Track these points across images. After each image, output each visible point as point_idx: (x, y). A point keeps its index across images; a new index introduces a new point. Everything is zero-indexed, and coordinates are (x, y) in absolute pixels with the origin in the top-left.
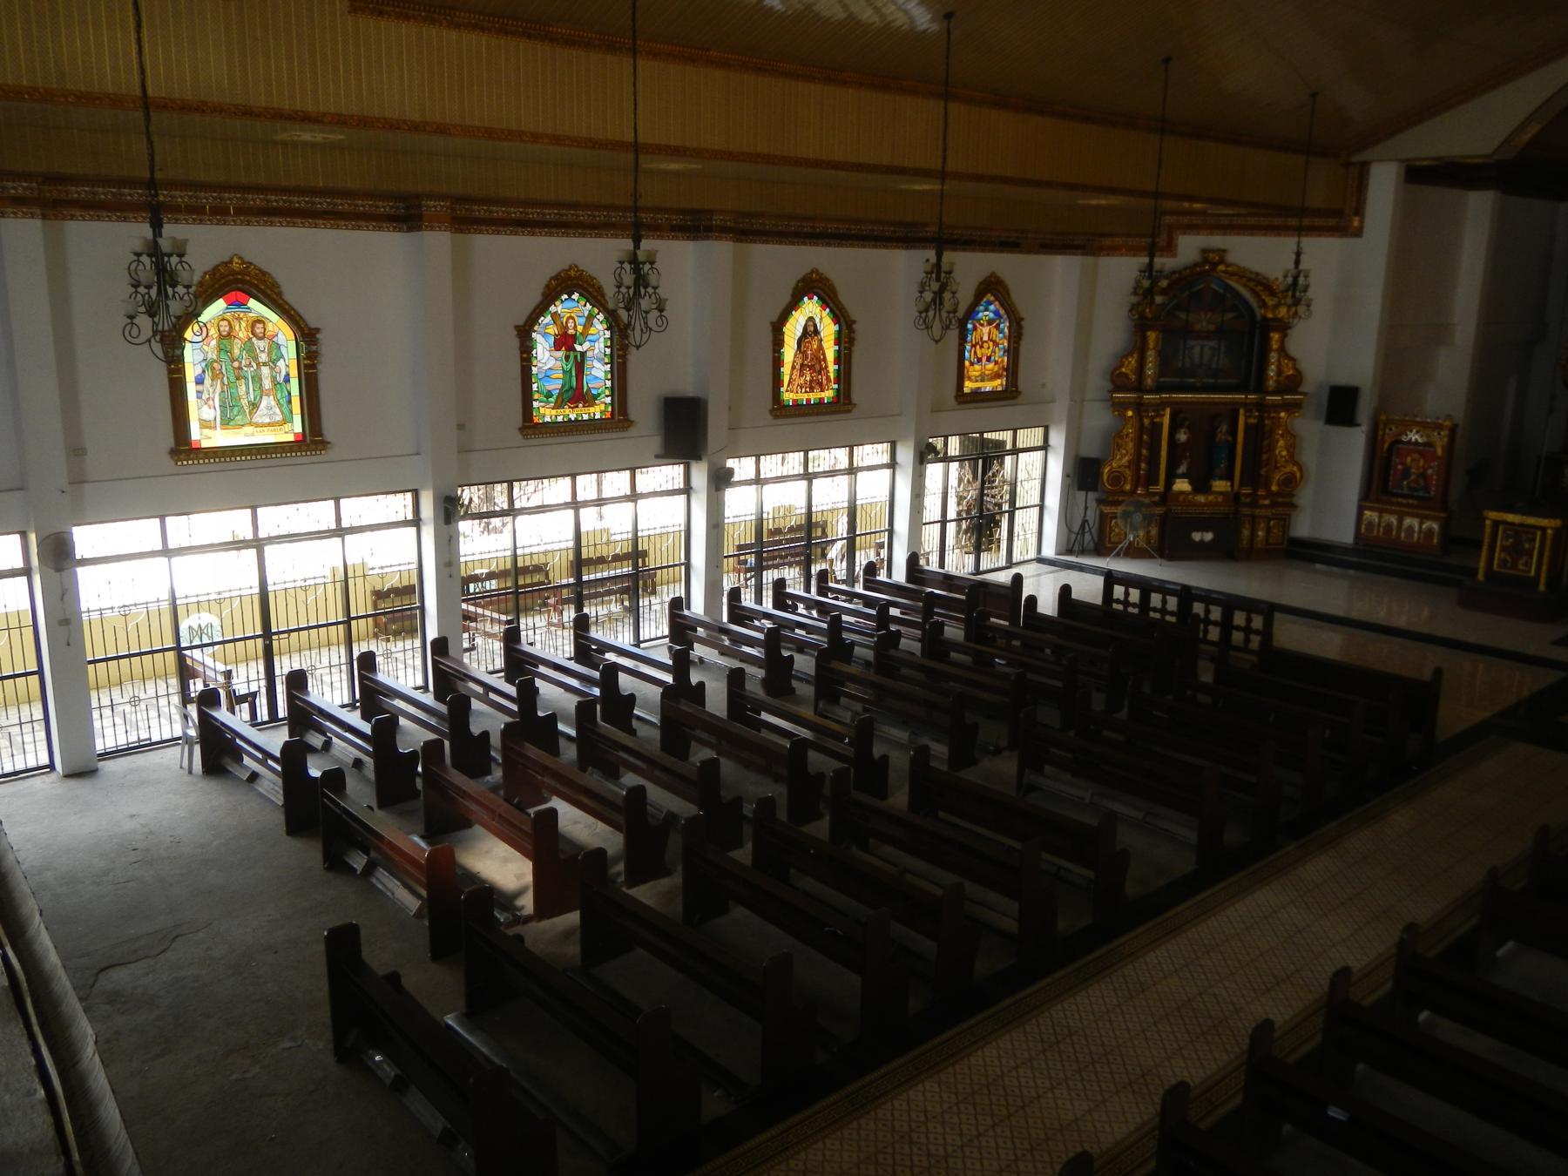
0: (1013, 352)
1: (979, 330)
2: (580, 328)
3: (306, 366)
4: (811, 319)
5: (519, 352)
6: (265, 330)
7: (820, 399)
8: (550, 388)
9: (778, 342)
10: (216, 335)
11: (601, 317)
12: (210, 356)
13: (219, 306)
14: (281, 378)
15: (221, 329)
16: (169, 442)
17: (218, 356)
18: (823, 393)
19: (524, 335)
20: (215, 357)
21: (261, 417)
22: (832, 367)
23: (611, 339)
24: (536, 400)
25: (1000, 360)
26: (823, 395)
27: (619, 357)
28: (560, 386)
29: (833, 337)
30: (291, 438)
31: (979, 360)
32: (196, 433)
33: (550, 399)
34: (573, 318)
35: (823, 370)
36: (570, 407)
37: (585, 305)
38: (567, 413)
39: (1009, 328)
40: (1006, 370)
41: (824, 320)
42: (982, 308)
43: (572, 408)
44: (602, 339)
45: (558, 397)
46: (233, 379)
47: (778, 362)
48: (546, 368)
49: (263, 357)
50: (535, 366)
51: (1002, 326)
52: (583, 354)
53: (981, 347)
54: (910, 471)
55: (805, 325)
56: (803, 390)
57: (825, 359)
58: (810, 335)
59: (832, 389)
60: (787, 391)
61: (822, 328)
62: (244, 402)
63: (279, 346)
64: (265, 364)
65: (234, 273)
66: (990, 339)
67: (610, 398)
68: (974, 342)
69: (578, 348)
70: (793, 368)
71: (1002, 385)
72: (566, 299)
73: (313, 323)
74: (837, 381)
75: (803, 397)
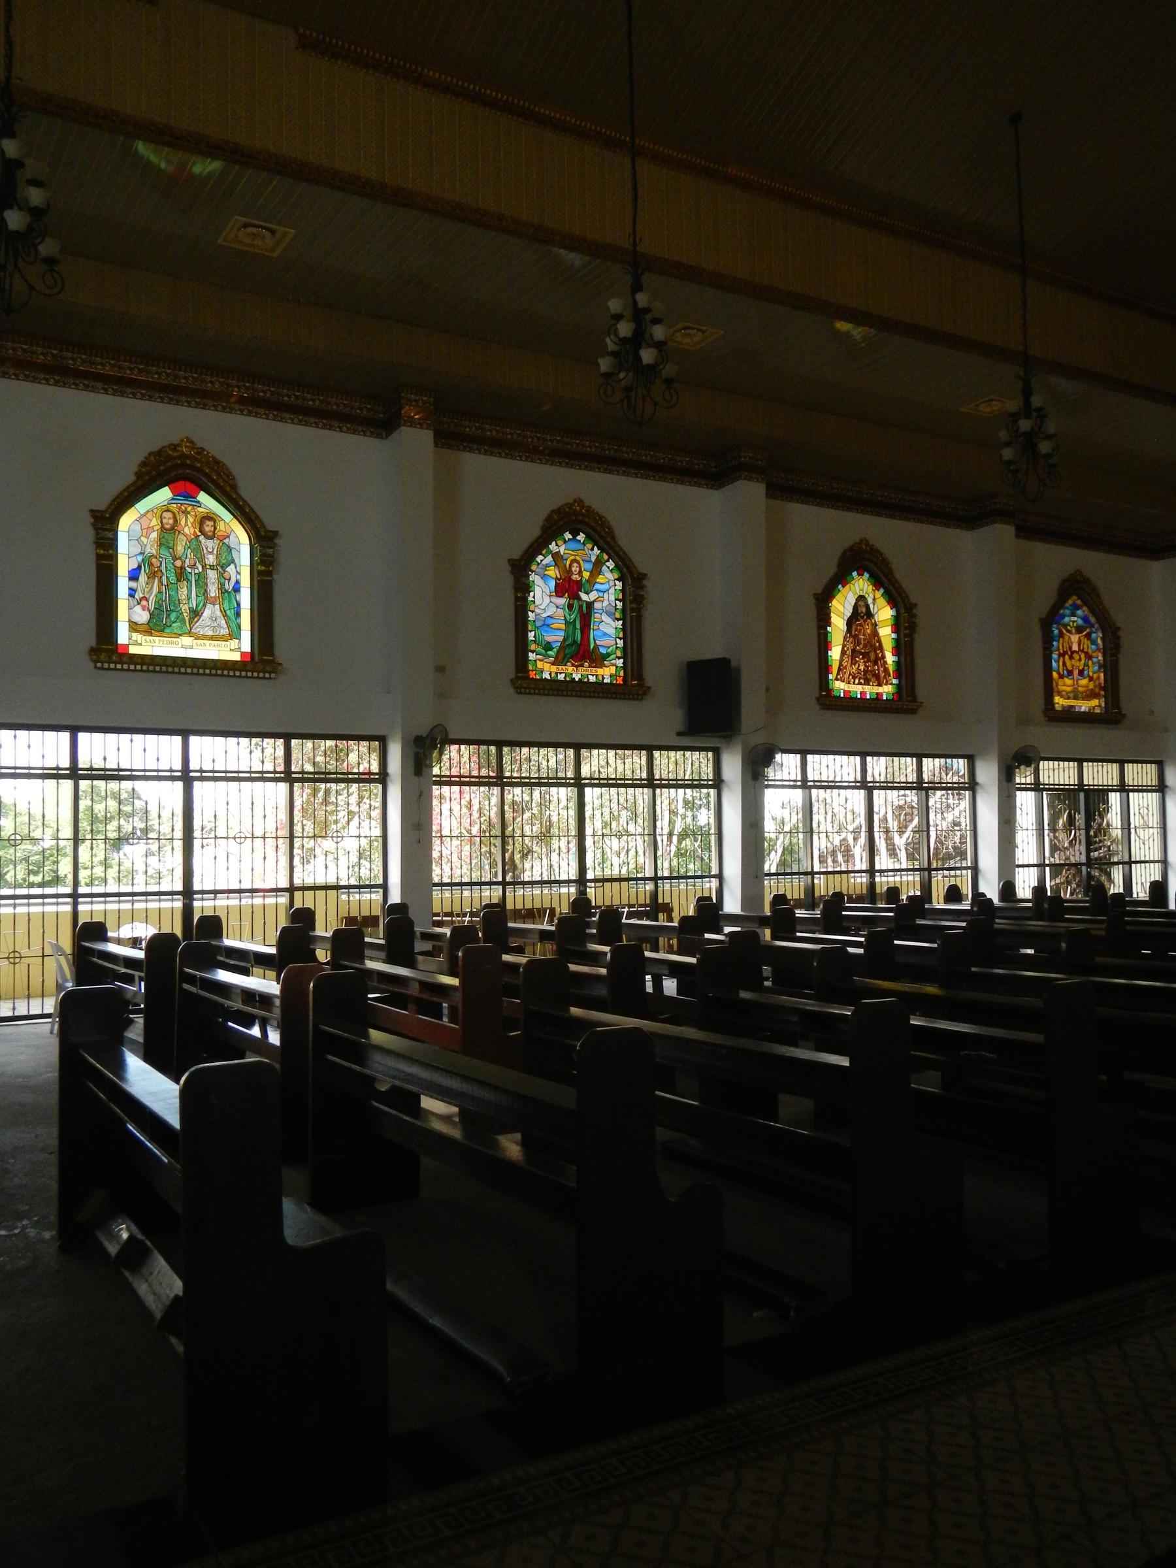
0: (1111, 667)
1: (1066, 638)
3: (260, 573)
4: (861, 598)
5: (513, 591)
6: (215, 529)
7: (877, 694)
8: (550, 639)
9: (824, 619)
10: (158, 527)
11: (611, 564)
12: (148, 550)
13: (164, 494)
14: (229, 587)
15: (165, 521)
16: (91, 640)
17: (158, 551)
19: (520, 570)
20: (154, 552)
21: (203, 627)
22: (890, 659)
23: (623, 591)
25: (1095, 676)
26: (881, 690)
27: (632, 610)
28: (561, 639)
29: (891, 622)
30: (236, 657)
31: (1070, 673)
32: (123, 635)
33: (549, 653)
34: (578, 562)
36: (573, 665)
37: (592, 549)
38: (570, 671)
39: (1103, 639)
40: (1104, 689)
42: (1067, 612)
43: (577, 667)
44: (612, 591)
45: (558, 652)
46: (173, 579)
47: (824, 645)
48: (545, 615)
49: (211, 559)
50: (532, 612)
51: (1094, 635)
52: (590, 605)
53: (1071, 658)
54: (994, 790)
55: (856, 604)
56: (857, 681)
57: (881, 647)
58: (862, 617)
59: (891, 684)
60: (837, 679)
63: (230, 549)
64: (212, 567)
65: (184, 456)
66: (1081, 650)
67: (622, 660)
69: (584, 597)
70: (843, 653)
71: (1100, 706)
72: (569, 539)
73: (271, 526)
74: (898, 673)
75: (856, 689)
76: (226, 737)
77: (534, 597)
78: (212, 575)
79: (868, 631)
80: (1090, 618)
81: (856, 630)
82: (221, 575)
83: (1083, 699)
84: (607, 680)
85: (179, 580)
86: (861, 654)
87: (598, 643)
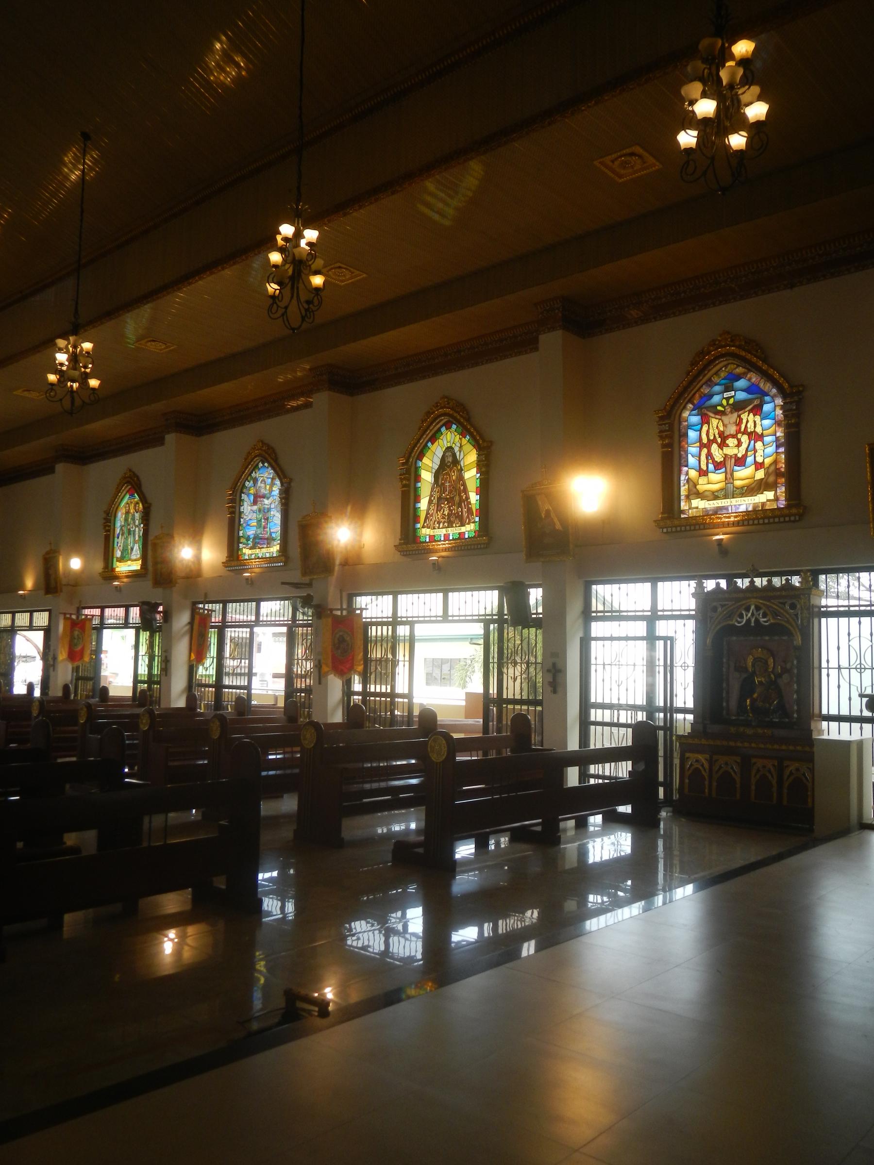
4: (450, 449)
7: (460, 534)
18: (462, 528)
21: (133, 555)
22: (474, 498)
24: (241, 543)
26: (463, 529)
38: (257, 552)
41: (464, 448)
50: (242, 518)
57: (465, 490)
58: (449, 467)
59: (474, 522)
60: (423, 527)
61: (462, 457)
62: (129, 547)
70: (430, 502)
72: (261, 467)
77: (244, 509)
78: (137, 529)
79: (454, 478)
80: (761, 385)
81: (442, 480)
82: (139, 528)
83: (743, 495)
84: (275, 555)
85: (129, 535)
86: (446, 499)
87: (272, 530)
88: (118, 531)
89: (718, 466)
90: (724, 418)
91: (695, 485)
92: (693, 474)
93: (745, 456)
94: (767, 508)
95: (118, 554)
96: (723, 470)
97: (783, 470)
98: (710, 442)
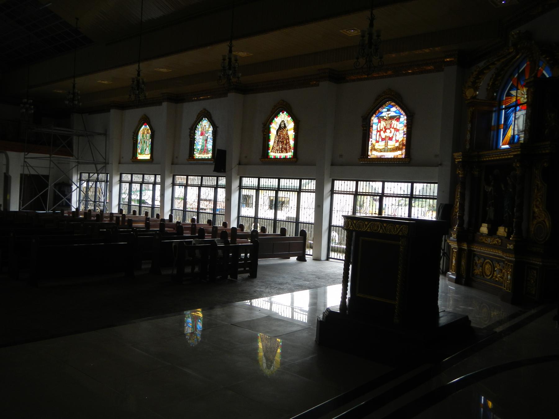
2: (207, 129)
4: (283, 121)
7: (285, 156)
9: (267, 132)
22: (292, 143)
26: (286, 154)
28: (201, 147)
33: (198, 151)
35: (288, 143)
42: (385, 110)
55: (280, 124)
56: (278, 152)
57: (288, 139)
58: (282, 128)
59: (292, 152)
60: (271, 152)
62: (144, 149)
68: (379, 129)
70: (275, 142)
75: (278, 155)
76: (350, 181)
78: (148, 141)
79: (284, 133)
81: (280, 134)
82: (149, 141)
83: (390, 151)
86: (281, 142)
88: (139, 141)
89: (383, 140)
90: (386, 121)
91: (374, 146)
92: (374, 142)
93: (392, 137)
94: (399, 157)
95: (139, 151)
96: (385, 141)
97: (405, 143)
98: (381, 130)
